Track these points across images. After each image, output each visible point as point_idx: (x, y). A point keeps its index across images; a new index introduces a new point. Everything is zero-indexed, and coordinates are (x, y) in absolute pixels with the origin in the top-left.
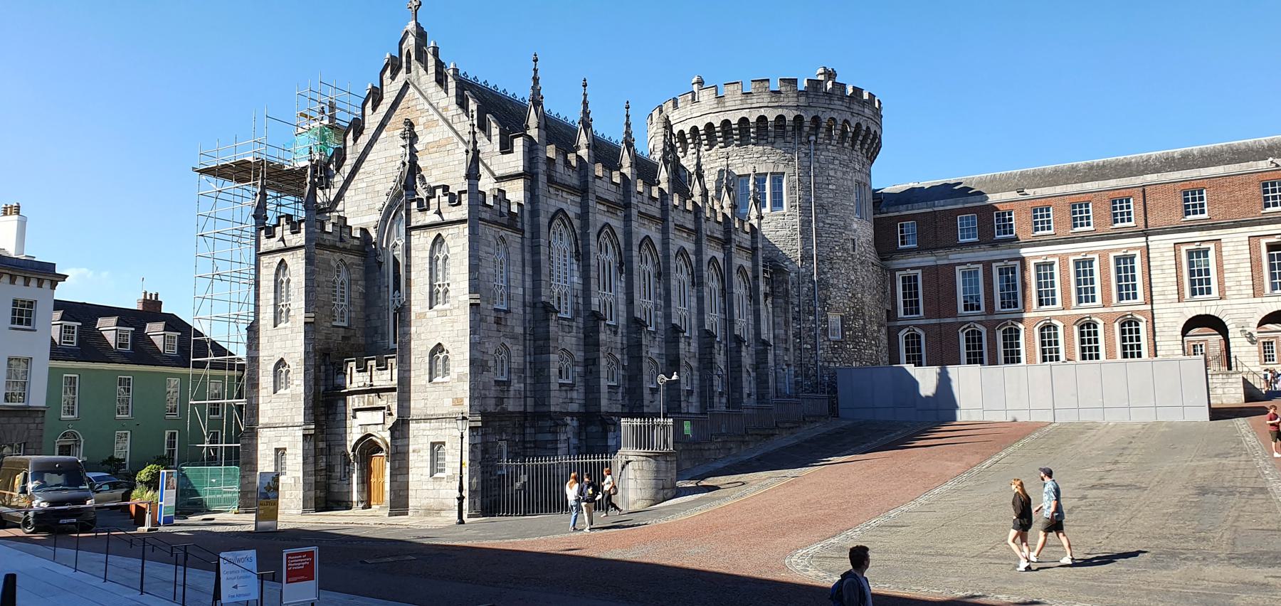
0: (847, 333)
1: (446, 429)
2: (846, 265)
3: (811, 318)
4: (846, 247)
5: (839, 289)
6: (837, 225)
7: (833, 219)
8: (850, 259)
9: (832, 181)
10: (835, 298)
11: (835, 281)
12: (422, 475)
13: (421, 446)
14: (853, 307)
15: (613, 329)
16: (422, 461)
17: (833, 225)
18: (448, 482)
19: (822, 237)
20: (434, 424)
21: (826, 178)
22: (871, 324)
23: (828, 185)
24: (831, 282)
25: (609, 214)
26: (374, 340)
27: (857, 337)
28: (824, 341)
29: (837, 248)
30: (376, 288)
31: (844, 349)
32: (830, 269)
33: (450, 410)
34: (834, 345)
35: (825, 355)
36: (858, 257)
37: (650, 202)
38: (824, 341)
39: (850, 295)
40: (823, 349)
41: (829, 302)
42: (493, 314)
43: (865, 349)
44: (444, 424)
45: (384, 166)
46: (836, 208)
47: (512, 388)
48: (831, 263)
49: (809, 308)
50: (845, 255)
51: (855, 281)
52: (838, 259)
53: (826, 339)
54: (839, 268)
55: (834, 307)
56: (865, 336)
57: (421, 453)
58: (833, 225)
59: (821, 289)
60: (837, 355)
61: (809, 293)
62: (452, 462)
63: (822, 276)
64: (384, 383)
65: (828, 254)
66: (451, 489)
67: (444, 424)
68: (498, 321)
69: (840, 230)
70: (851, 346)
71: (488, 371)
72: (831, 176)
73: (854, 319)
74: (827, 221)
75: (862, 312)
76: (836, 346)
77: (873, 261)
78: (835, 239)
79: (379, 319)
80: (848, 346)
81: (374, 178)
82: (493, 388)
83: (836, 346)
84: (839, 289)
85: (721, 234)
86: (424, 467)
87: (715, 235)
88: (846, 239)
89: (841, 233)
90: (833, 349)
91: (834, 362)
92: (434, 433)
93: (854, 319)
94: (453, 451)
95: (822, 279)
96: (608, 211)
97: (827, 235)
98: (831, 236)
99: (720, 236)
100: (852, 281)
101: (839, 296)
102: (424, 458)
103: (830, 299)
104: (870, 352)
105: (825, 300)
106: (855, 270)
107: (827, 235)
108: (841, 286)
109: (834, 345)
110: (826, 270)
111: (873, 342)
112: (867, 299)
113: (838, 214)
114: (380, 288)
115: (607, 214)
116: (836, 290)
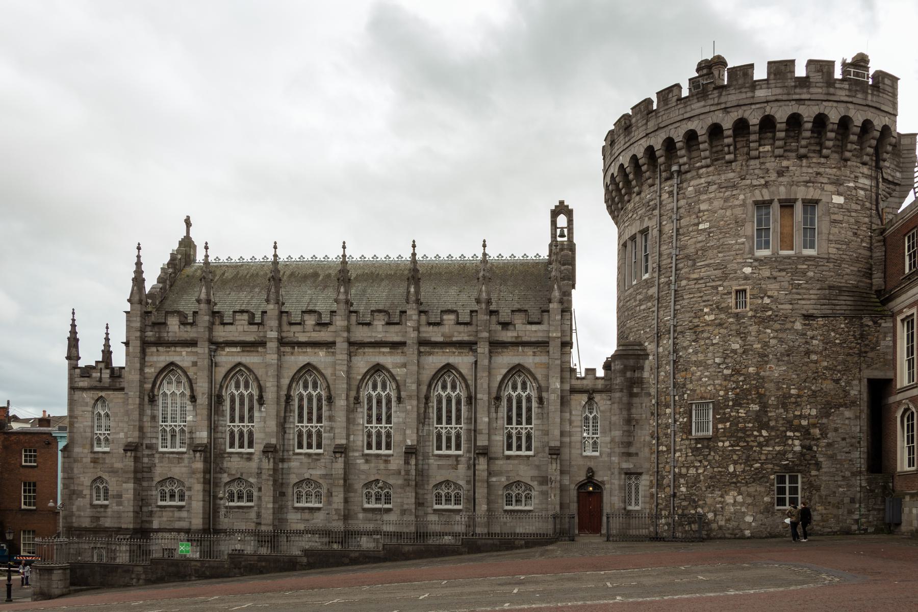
0: (720, 426)
2: (722, 331)
3: (668, 411)
4: (723, 305)
5: (707, 367)
6: (709, 276)
7: (703, 270)
8: (731, 320)
9: (704, 218)
10: (700, 379)
11: (701, 357)
14: (734, 388)
15: (245, 456)
17: (702, 278)
19: (683, 299)
21: (694, 216)
22: (784, 406)
23: (698, 224)
24: (694, 358)
25: (246, 354)
27: (744, 430)
28: (682, 440)
29: (706, 310)
31: (715, 449)
32: (694, 341)
34: (696, 443)
35: (683, 459)
36: (750, 314)
37: (317, 328)
38: (682, 440)
39: (727, 372)
40: (680, 450)
41: (690, 386)
42: (90, 455)
43: (760, 445)
46: (710, 253)
47: (109, 510)
48: (695, 332)
49: (665, 399)
50: (723, 316)
51: (741, 351)
52: (708, 325)
53: (684, 437)
54: (709, 338)
55: (698, 391)
56: (765, 426)
58: (702, 278)
59: (680, 371)
60: (699, 458)
61: (666, 379)
63: (681, 354)
65: (691, 322)
68: (95, 461)
69: (714, 284)
70: (727, 444)
71: (83, 498)
72: (703, 211)
73: (734, 405)
74: (695, 276)
75: (758, 393)
76: (699, 446)
77: (811, 312)
78: (705, 298)
80: (720, 444)
82: (88, 510)
83: (699, 446)
84: (707, 367)
85: (469, 336)
87: (454, 339)
88: (725, 294)
89: (716, 287)
90: (695, 450)
91: (695, 467)
93: (737, 403)
95: (681, 357)
96: (243, 351)
97: (692, 296)
98: (699, 295)
99: (466, 338)
100: (734, 351)
101: (706, 376)
103: (691, 383)
104: (777, 448)
105: (684, 385)
106: (742, 335)
107: (692, 296)
108: (710, 362)
109: (696, 443)
110: (686, 344)
111: (789, 434)
112: (775, 371)
113: (712, 261)
115: (242, 354)
116: (700, 368)
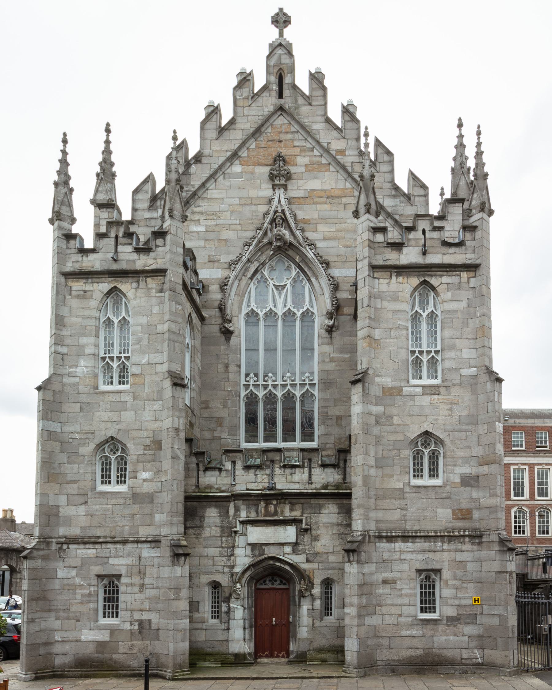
1: (443, 550)
12: (400, 616)
13: (397, 575)
16: (401, 596)
18: (448, 625)
20: (420, 544)
26: (216, 434)
30: (221, 368)
33: (449, 525)
44: (439, 544)
45: (237, 208)
57: (399, 585)
62: (457, 598)
64: (296, 486)
66: (455, 635)
67: (439, 544)
79: (225, 407)
81: (219, 222)
86: (404, 605)
92: (420, 556)
94: (455, 582)
102: (403, 592)
114: (227, 367)
